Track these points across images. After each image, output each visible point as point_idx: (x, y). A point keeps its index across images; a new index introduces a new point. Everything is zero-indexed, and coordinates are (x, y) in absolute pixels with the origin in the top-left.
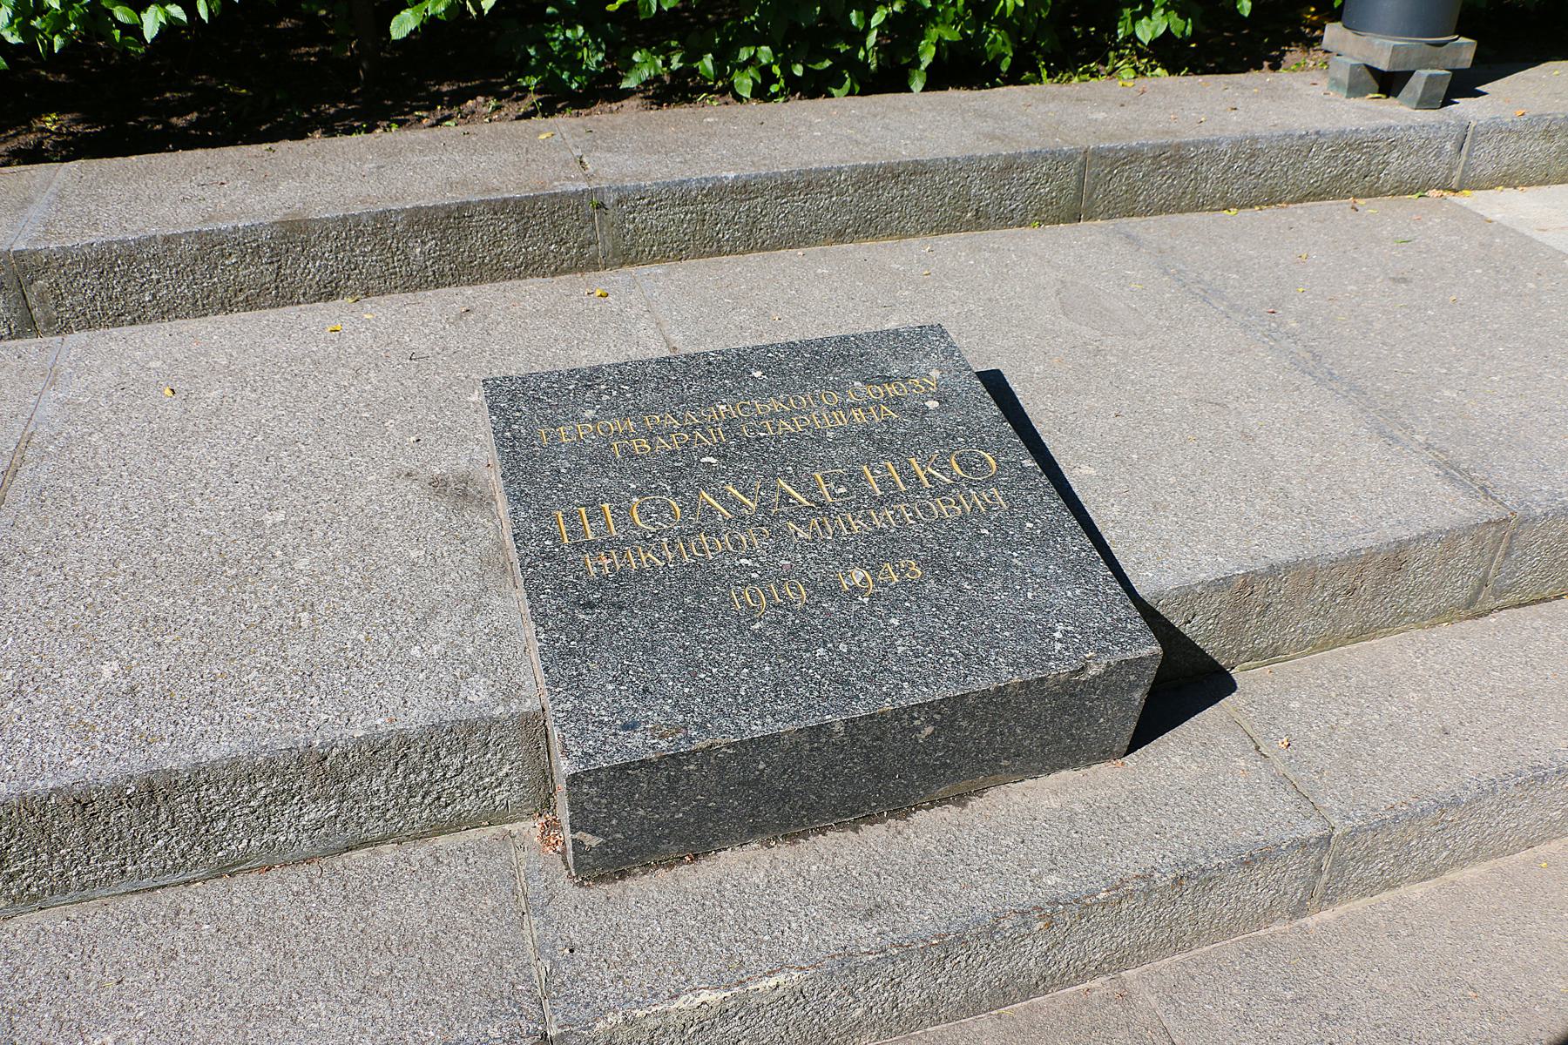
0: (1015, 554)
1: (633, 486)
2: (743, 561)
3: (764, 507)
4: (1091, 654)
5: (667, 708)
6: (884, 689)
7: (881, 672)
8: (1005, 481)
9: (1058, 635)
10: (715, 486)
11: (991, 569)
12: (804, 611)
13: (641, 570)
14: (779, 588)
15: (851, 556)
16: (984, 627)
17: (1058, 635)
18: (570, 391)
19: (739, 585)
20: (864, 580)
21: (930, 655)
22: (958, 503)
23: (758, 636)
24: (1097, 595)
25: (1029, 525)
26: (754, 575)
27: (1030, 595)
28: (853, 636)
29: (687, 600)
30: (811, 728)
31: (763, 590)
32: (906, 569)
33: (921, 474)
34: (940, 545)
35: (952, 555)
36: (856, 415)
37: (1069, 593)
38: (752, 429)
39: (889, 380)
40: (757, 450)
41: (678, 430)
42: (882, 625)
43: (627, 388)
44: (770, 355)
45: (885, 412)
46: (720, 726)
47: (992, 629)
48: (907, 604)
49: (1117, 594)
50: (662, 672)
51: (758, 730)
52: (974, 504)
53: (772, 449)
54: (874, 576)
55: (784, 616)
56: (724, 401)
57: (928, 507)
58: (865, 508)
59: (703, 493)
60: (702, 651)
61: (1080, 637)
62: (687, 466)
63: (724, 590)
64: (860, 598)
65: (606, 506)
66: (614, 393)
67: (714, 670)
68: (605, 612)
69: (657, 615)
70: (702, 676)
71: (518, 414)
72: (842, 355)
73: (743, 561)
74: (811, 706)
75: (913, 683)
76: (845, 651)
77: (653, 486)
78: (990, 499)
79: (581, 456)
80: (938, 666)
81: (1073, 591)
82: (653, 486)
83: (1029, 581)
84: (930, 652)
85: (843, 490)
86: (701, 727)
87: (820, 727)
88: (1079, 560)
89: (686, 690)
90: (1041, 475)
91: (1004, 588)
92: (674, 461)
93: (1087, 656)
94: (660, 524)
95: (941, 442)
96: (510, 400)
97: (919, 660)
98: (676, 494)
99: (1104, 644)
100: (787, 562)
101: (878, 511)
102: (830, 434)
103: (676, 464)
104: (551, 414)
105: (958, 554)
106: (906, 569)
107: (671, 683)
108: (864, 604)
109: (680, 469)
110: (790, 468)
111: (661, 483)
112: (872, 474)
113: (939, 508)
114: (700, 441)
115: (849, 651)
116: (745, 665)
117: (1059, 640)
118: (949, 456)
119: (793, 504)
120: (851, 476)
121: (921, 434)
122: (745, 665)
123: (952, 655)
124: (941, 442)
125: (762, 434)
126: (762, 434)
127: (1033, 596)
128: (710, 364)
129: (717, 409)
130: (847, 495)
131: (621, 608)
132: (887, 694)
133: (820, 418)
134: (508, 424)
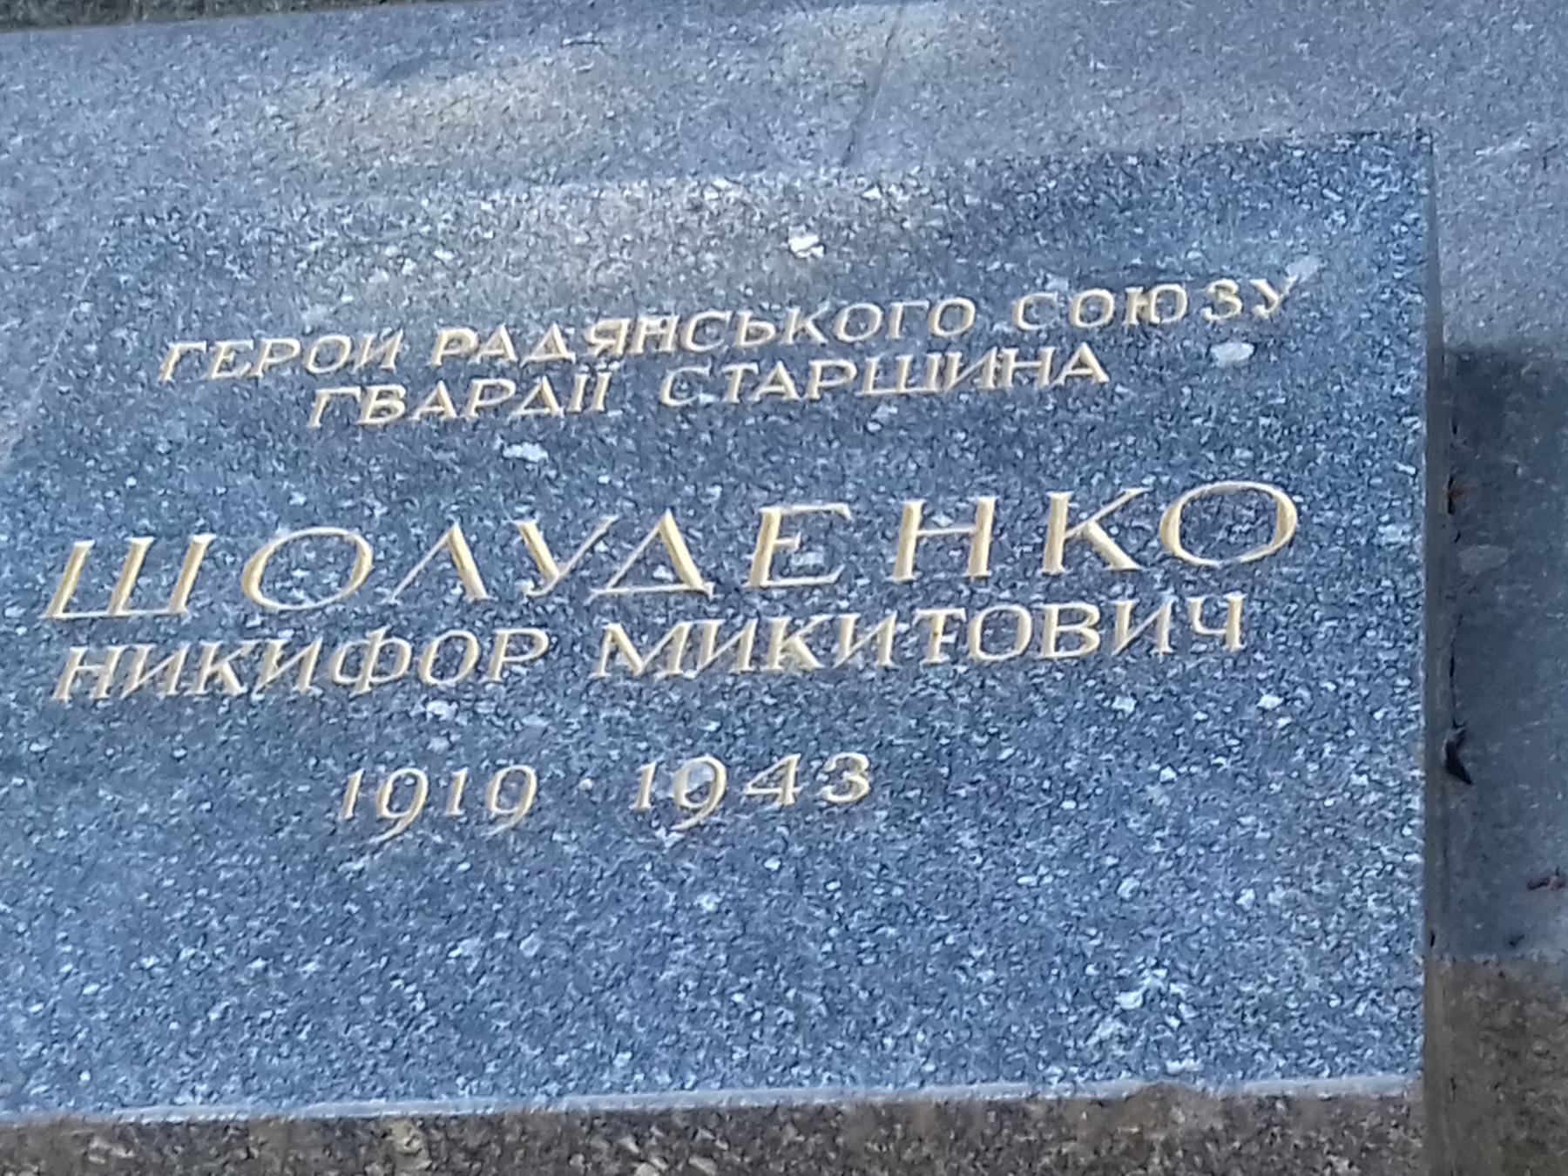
0: (1168, 774)
1: (299, 499)
2: (439, 708)
3: (576, 584)
4: (1189, 1063)
5: (19, 1023)
6: (561, 1060)
7: (584, 1018)
8: (1291, 579)
9: (1130, 1000)
10: (497, 520)
11: (1069, 805)
12: (496, 844)
13: (178, 700)
14: (478, 779)
15: (713, 726)
16: (938, 947)
17: (1130, 1000)
18: (304, 253)
19: (384, 762)
20: (704, 791)
21: (738, 998)
22: (1107, 621)
23: (343, 889)
24: (1325, 913)
25: (1269, 701)
26: (438, 744)
27: (1127, 886)
28: (575, 922)
29: (236, 782)
30: (326, 1125)
31: (433, 784)
32: (834, 776)
33: (1059, 535)
34: (972, 725)
35: (983, 755)
36: (993, 364)
37: (1248, 896)
38: (692, 384)
39: (1149, 277)
40: (665, 437)
41: (502, 373)
42: (669, 905)
43: (446, 256)
44: (874, 193)
45: (1082, 364)
46: (109, 1082)
47: (954, 957)
48: (773, 864)
49: (1388, 919)
50: (65, 940)
51: (192, 1108)
52: (1152, 630)
53: (706, 437)
54: (735, 781)
55: (440, 850)
56: (668, 304)
57: (1014, 622)
58: (839, 610)
59: (456, 529)
60: (190, 904)
61: (1187, 1013)
62: (463, 462)
63: (338, 770)
64: (661, 833)
65: (204, 539)
66: (409, 267)
67: (186, 953)
68: (31, 785)
69: (144, 808)
70: (148, 962)
71: (146, 303)
72: (1069, 207)
73: (439, 708)
74: (353, 1071)
75: (642, 1058)
76: (531, 953)
77: (349, 503)
78: (1207, 621)
79: (223, 418)
80: (739, 1025)
81: (1262, 891)
82: (349, 503)
83: (1157, 848)
84: (745, 990)
85: (812, 559)
86: (66, 1078)
87: (347, 1127)
88: (1342, 816)
89: (91, 989)
90: (1412, 569)
91: (1068, 858)
92: (437, 448)
93: (1173, 1066)
94: (300, 595)
95: (1181, 456)
96: (149, 266)
97: (702, 1005)
98: (386, 528)
99: (1244, 1044)
100: (542, 723)
101: (868, 619)
102: (883, 412)
103: (440, 456)
104: (223, 308)
105: (1005, 755)
106: (834, 776)
107: (66, 968)
108: (659, 847)
109: (437, 468)
110: (717, 490)
111: (370, 500)
112: (922, 525)
113: (1038, 633)
114: (539, 401)
115: (539, 957)
116: (264, 953)
117: (1124, 1015)
118: (1172, 493)
119: (661, 581)
120: (859, 526)
121: (1139, 431)
122: (264, 953)
123: (797, 1005)
124: (1181, 456)
125: (706, 398)
126: (706, 398)
127: (1135, 892)
128: (697, 208)
129: (633, 329)
130: (818, 570)
131: (74, 780)
132: (560, 1076)
133: (888, 368)
134: (108, 326)
